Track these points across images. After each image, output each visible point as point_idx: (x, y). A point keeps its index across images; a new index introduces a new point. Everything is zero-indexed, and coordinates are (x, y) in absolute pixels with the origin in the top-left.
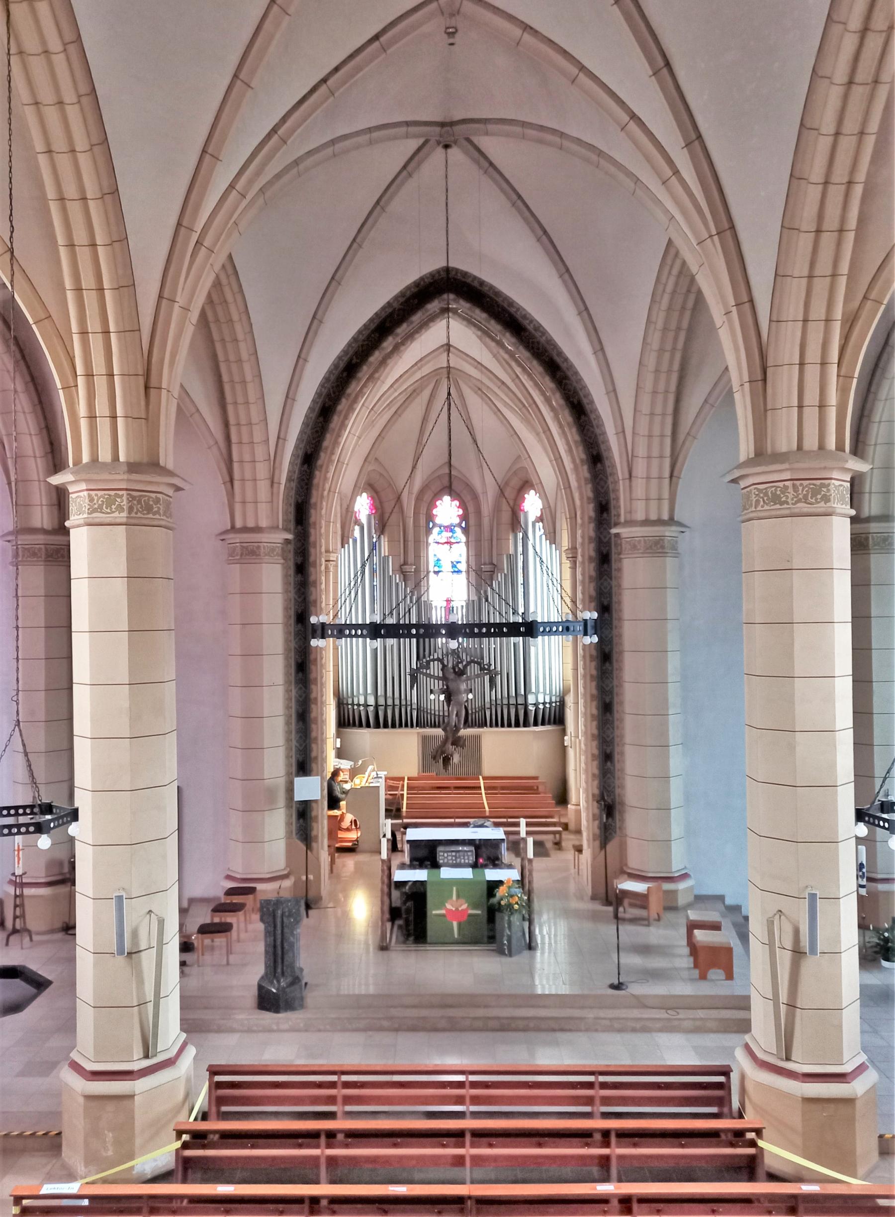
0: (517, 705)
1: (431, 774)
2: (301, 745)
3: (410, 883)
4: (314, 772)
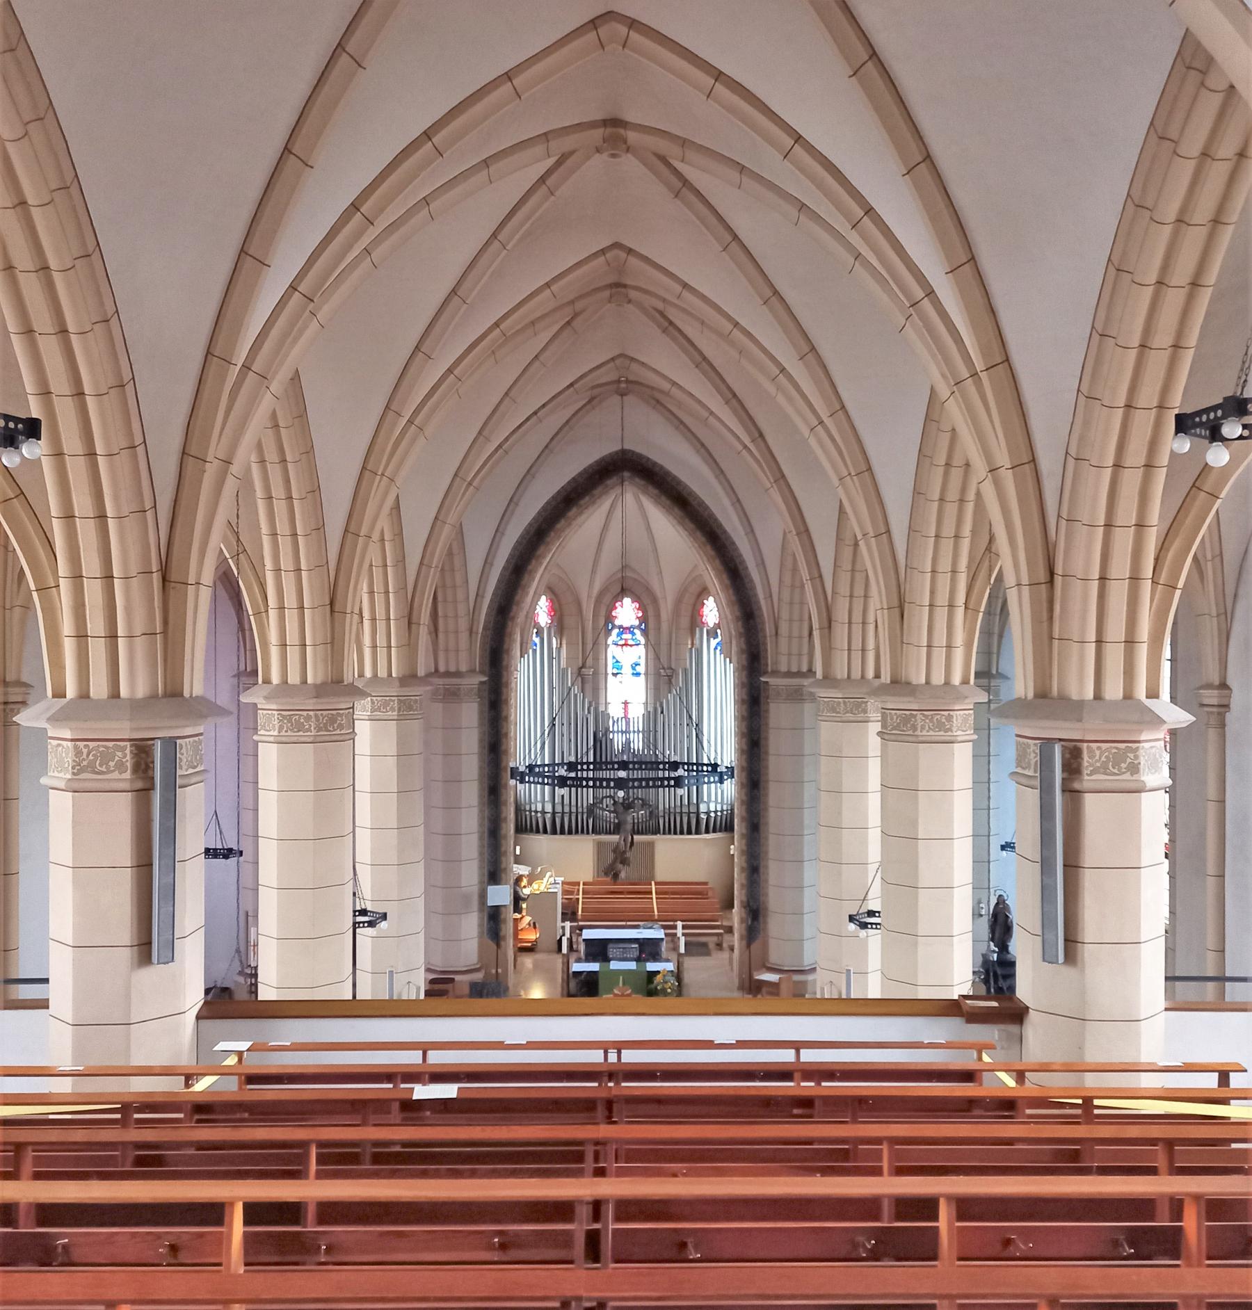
0: (689, 813)
2: (492, 858)
4: (504, 881)
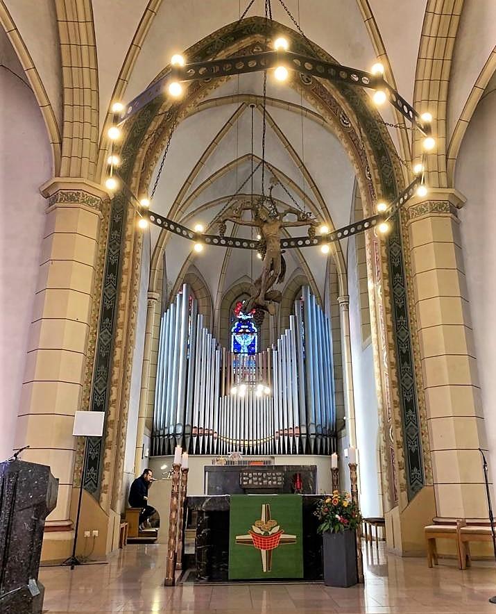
3: (207, 500)
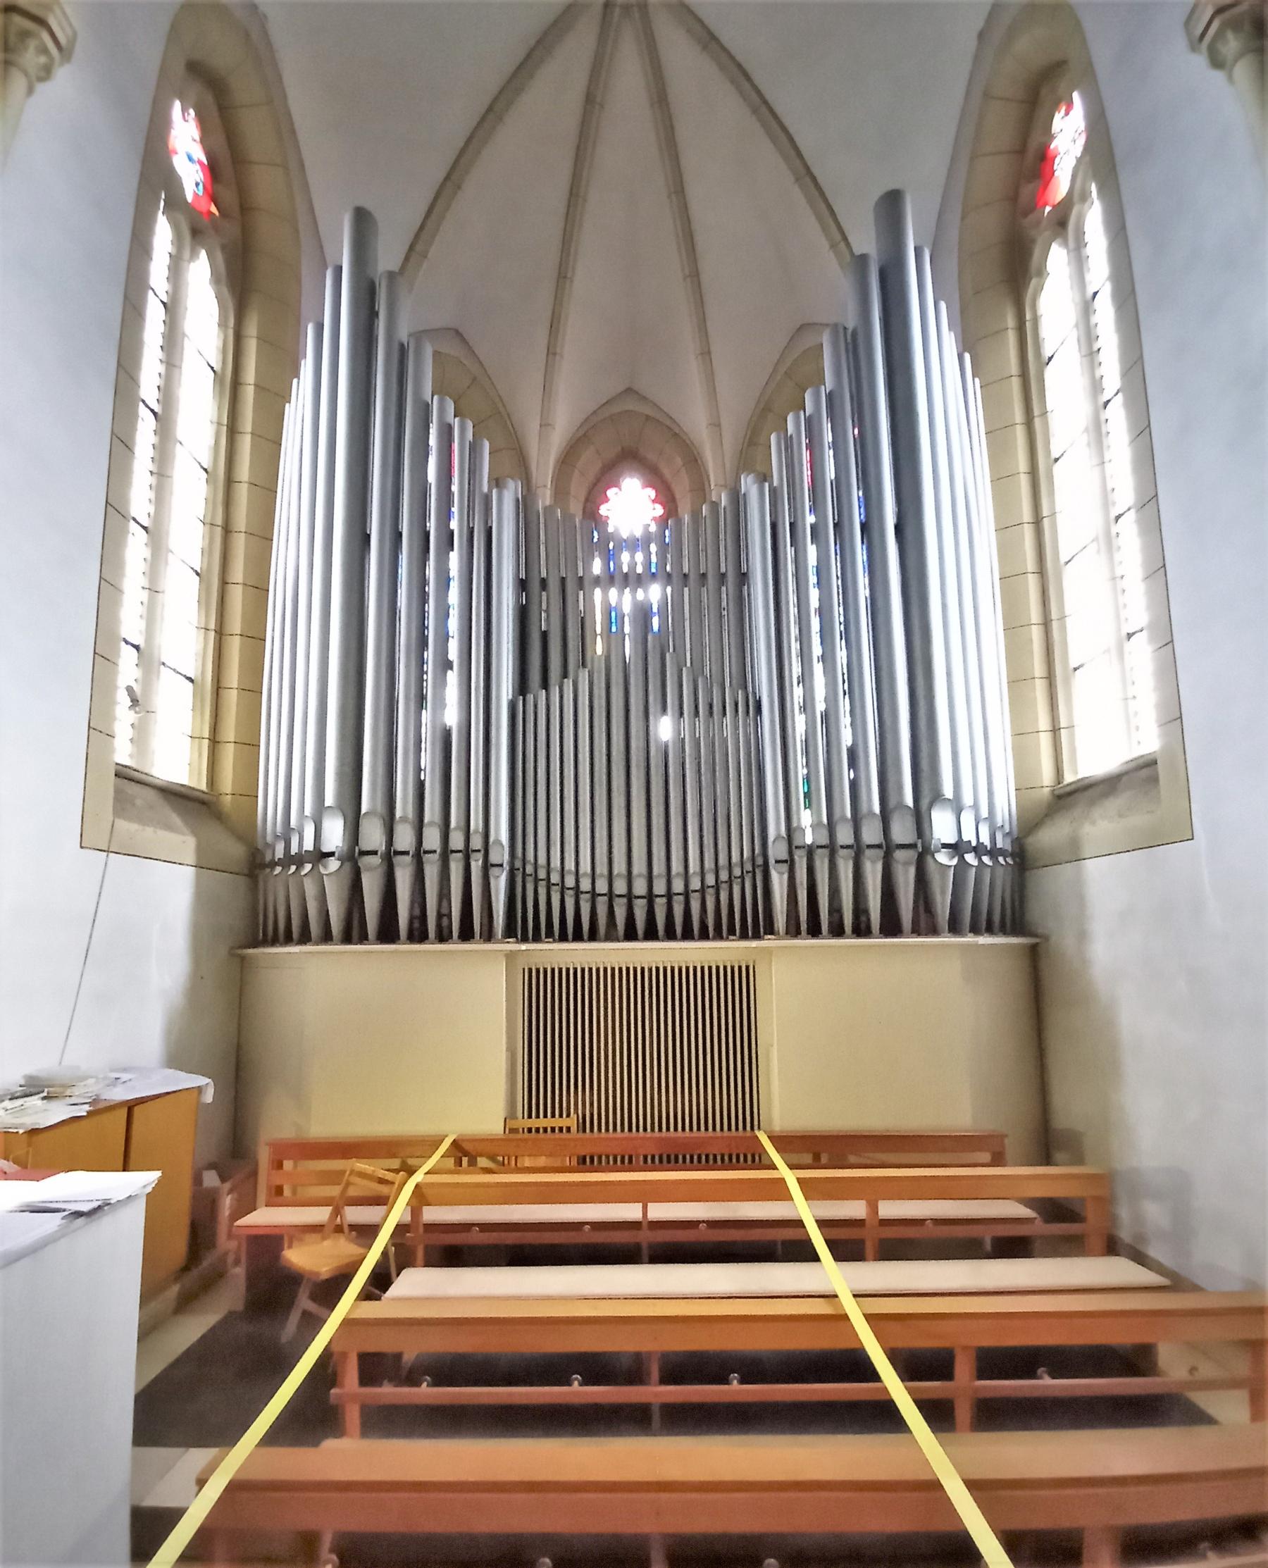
1: (558, 1122)
